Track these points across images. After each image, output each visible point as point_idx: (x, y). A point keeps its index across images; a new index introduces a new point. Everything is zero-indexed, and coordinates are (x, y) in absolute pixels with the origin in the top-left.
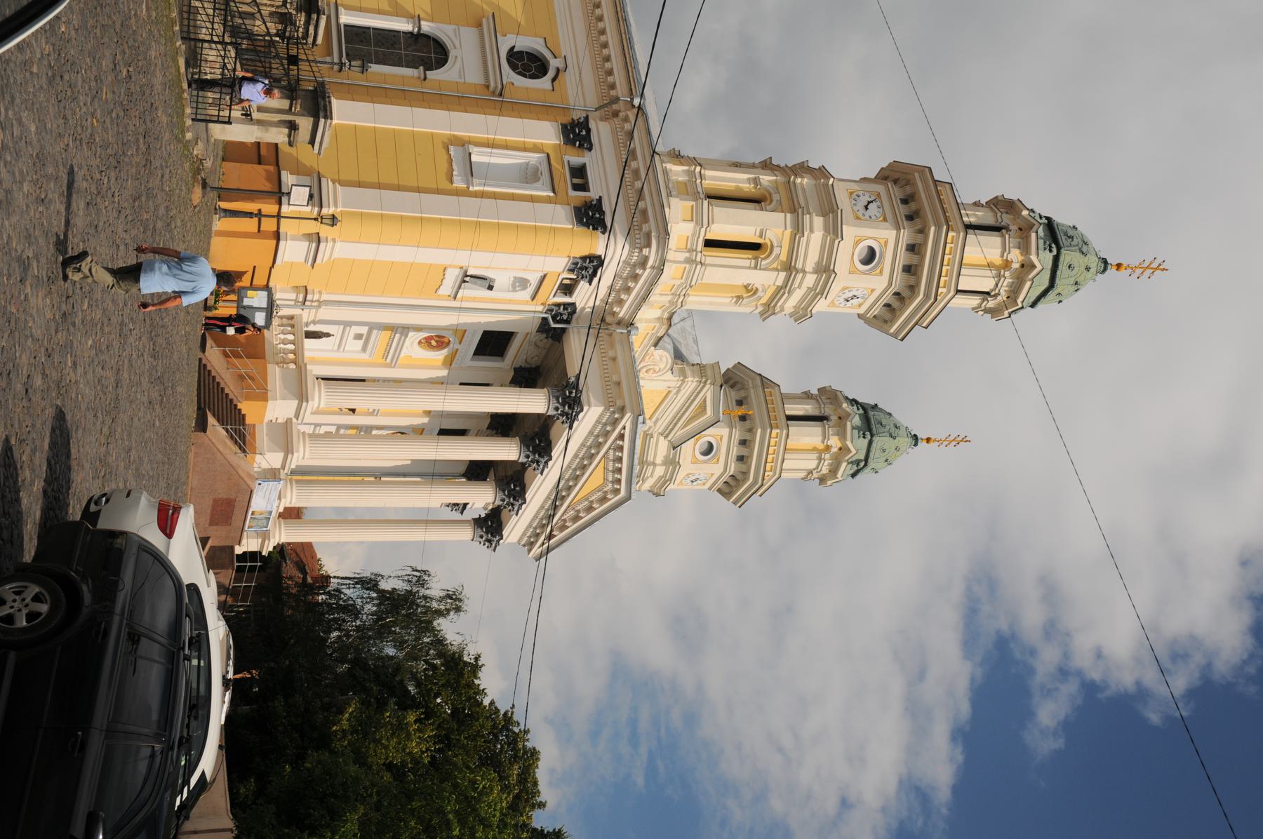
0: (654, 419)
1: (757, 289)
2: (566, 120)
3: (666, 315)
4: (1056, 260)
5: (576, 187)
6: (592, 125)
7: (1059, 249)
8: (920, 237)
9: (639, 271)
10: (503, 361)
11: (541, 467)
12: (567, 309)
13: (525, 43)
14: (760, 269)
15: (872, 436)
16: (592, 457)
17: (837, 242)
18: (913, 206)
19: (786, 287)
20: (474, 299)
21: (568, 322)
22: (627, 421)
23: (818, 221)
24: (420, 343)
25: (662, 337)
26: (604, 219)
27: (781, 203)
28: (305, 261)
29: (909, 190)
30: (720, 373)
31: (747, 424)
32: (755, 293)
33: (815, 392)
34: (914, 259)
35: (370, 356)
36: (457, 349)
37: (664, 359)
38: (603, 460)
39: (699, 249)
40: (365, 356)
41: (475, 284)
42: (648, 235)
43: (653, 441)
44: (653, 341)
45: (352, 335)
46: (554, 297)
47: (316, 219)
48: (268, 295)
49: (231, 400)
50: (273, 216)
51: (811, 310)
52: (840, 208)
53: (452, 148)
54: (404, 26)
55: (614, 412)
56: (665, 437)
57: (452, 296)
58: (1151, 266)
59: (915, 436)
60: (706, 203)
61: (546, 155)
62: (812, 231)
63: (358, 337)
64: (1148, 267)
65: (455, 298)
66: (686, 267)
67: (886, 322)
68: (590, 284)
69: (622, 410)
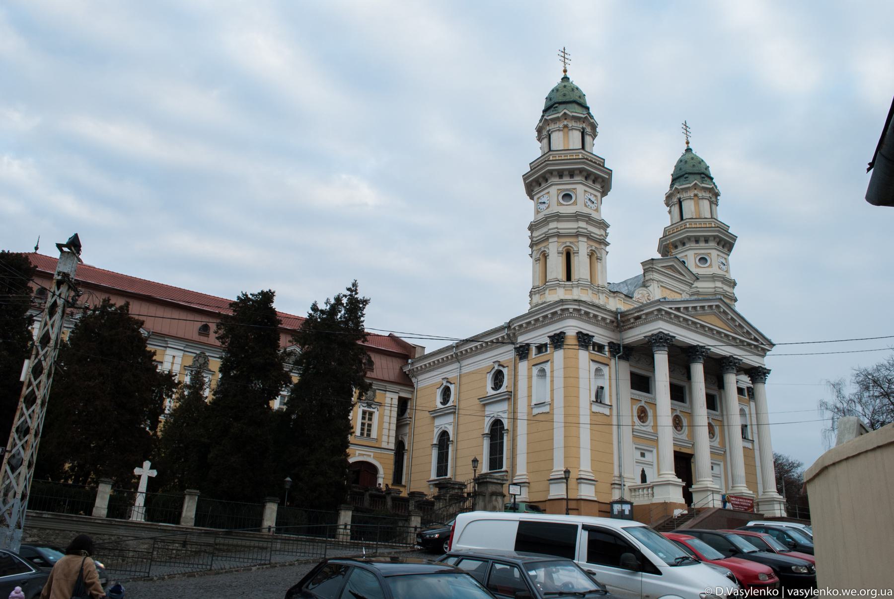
0: (681, 292)
1: (591, 250)
2: (518, 358)
3: (612, 295)
4: (560, 103)
5: (546, 351)
6: (518, 346)
7: (555, 103)
8: (554, 173)
9: (583, 312)
10: (651, 377)
11: (704, 350)
12: (611, 346)
13: (489, 384)
14: (578, 250)
15: (686, 174)
16: (694, 323)
17: (561, 215)
18: (541, 180)
20: (610, 396)
21: (619, 345)
22: (666, 308)
23: (553, 225)
24: (643, 422)
25: (625, 295)
26: (558, 334)
27: (545, 246)
28: (594, 485)
29: (534, 184)
30: (661, 259)
31: (686, 241)
32: (594, 251)
33: (669, 208)
34: (566, 173)
35: (655, 448)
36: (645, 402)
37: (640, 292)
38: (697, 317)
39: (571, 283)
40: (655, 451)
41: (601, 396)
42: (562, 310)
43: (701, 290)
44: (628, 299)
45: (642, 459)
46: (605, 354)
47: (567, 481)
48: (615, 503)
49: (671, 522)
50: (567, 503)
52: (544, 216)
53: (533, 414)
54: (486, 443)
55: (662, 315)
56: (692, 284)
57: (610, 407)
58: (563, 56)
59: (686, 150)
60: (547, 284)
61: (533, 368)
62: (557, 228)
63: (643, 455)
64: (564, 57)
65: (611, 406)
67: (603, 181)
68: (594, 336)
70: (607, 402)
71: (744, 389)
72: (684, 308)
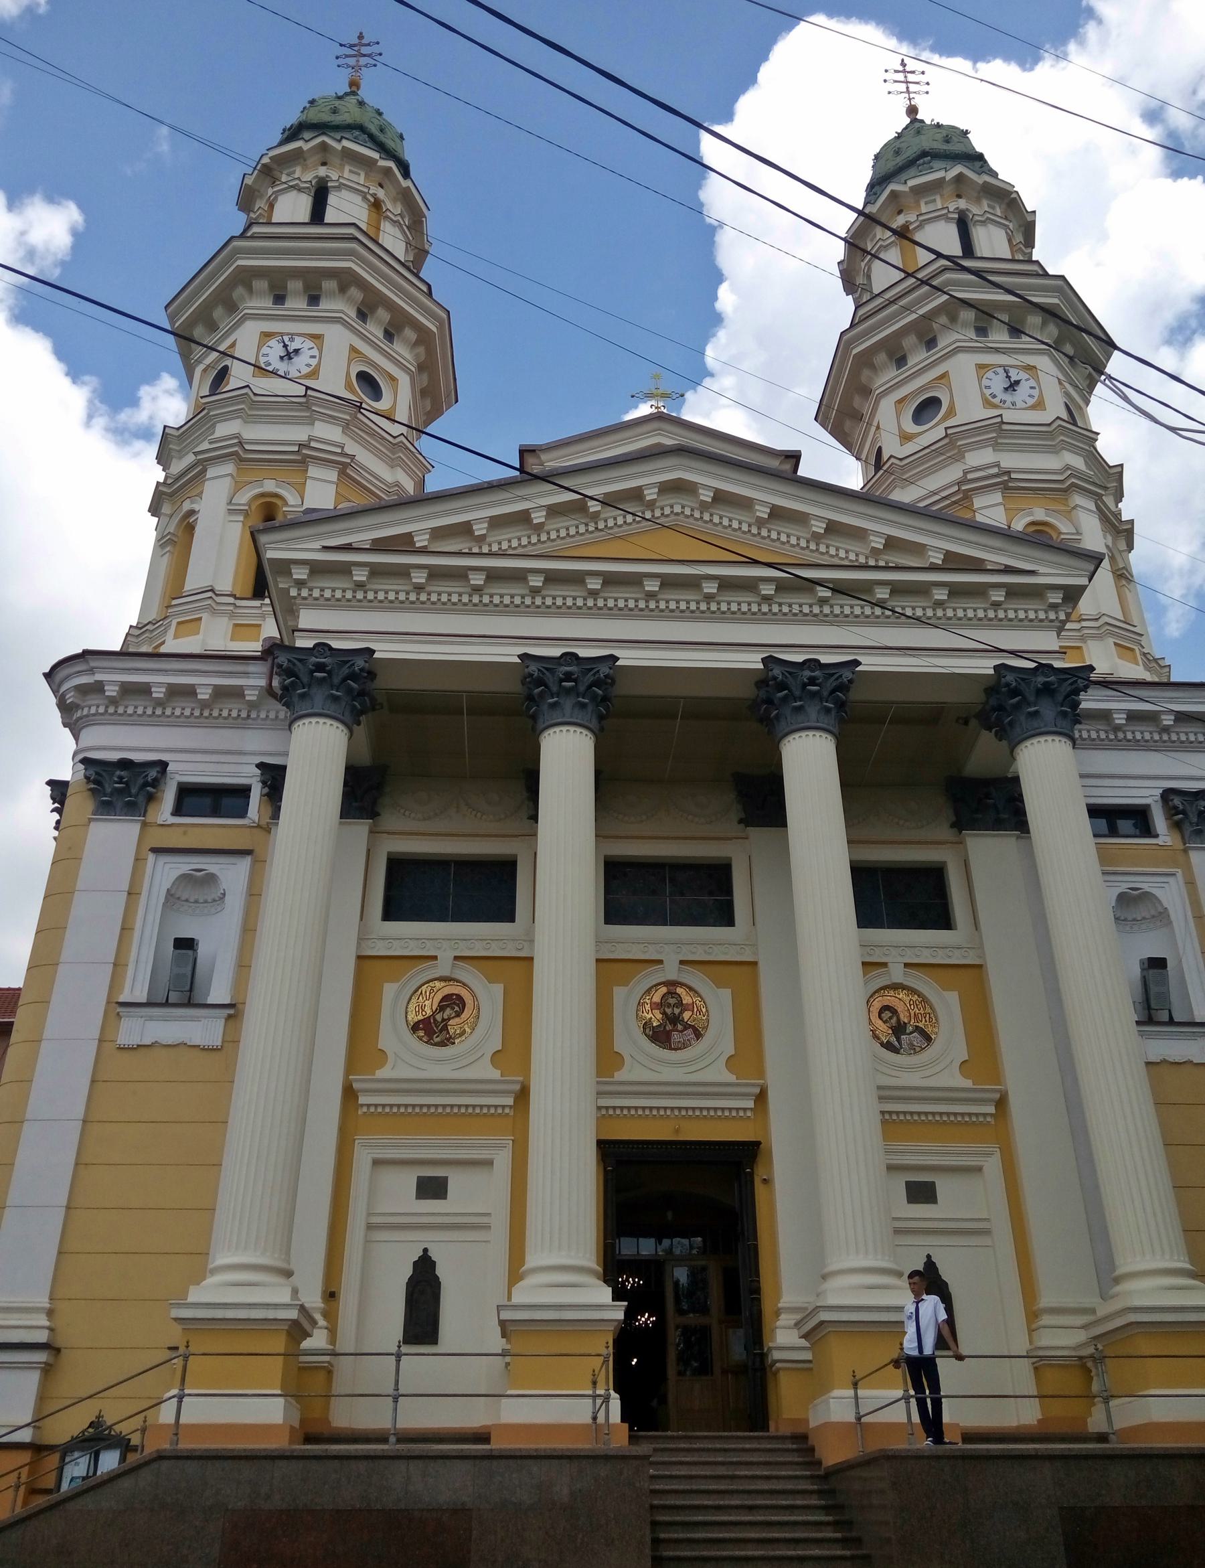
19: (231, 454)
20: (243, 967)
51: (305, 396)
55: (300, 584)
66: (179, 623)
71: (1148, 806)
72: (438, 533)
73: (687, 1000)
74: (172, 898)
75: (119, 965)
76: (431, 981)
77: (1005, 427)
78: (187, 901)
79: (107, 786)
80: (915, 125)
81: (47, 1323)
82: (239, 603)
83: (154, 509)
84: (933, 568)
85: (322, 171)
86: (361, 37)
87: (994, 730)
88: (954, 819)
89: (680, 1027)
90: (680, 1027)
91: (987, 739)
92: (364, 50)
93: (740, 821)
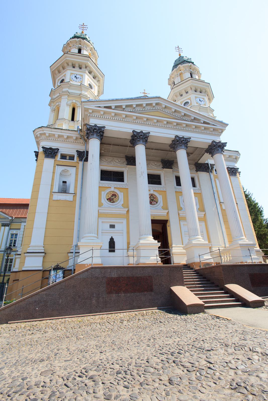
20: (76, 187)
21: (84, 152)
32: (75, 103)
36: (114, 188)
40: (125, 221)
55: (90, 113)
69: (86, 110)
70: (72, 190)
72: (116, 107)
73: (154, 197)
74: (61, 174)
75: (52, 186)
76: (110, 191)
77: (201, 107)
78: (63, 175)
79: (47, 152)
80: (181, 57)
81: (44, 249)
82: (70, 122)
83: (50, 105)
84: (202, 123)
85: (80, 45)
86: (83, 24)
87: (209, 153)
88: (196, 170)
89: (153, 201)
90: (153, 201)
91: (207, 155)
92: (84, 27)
93: (162, 168)
